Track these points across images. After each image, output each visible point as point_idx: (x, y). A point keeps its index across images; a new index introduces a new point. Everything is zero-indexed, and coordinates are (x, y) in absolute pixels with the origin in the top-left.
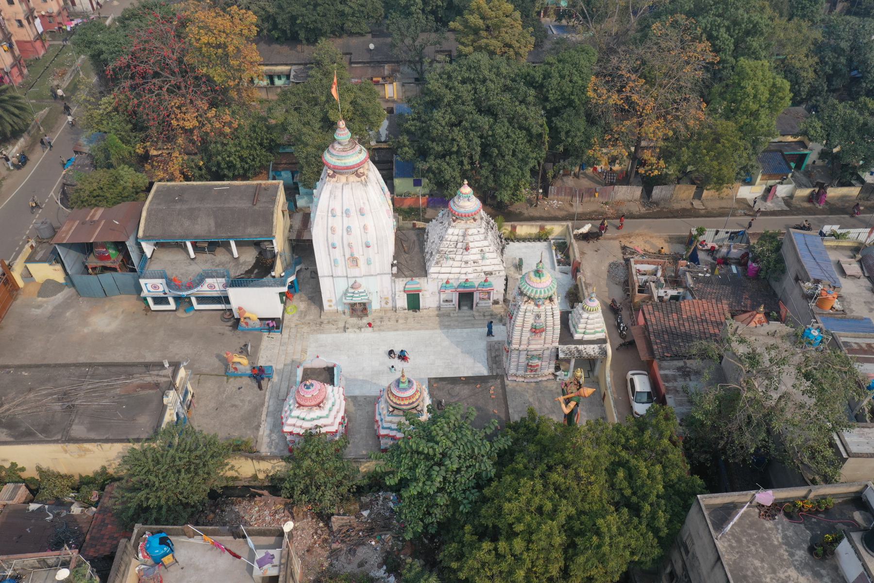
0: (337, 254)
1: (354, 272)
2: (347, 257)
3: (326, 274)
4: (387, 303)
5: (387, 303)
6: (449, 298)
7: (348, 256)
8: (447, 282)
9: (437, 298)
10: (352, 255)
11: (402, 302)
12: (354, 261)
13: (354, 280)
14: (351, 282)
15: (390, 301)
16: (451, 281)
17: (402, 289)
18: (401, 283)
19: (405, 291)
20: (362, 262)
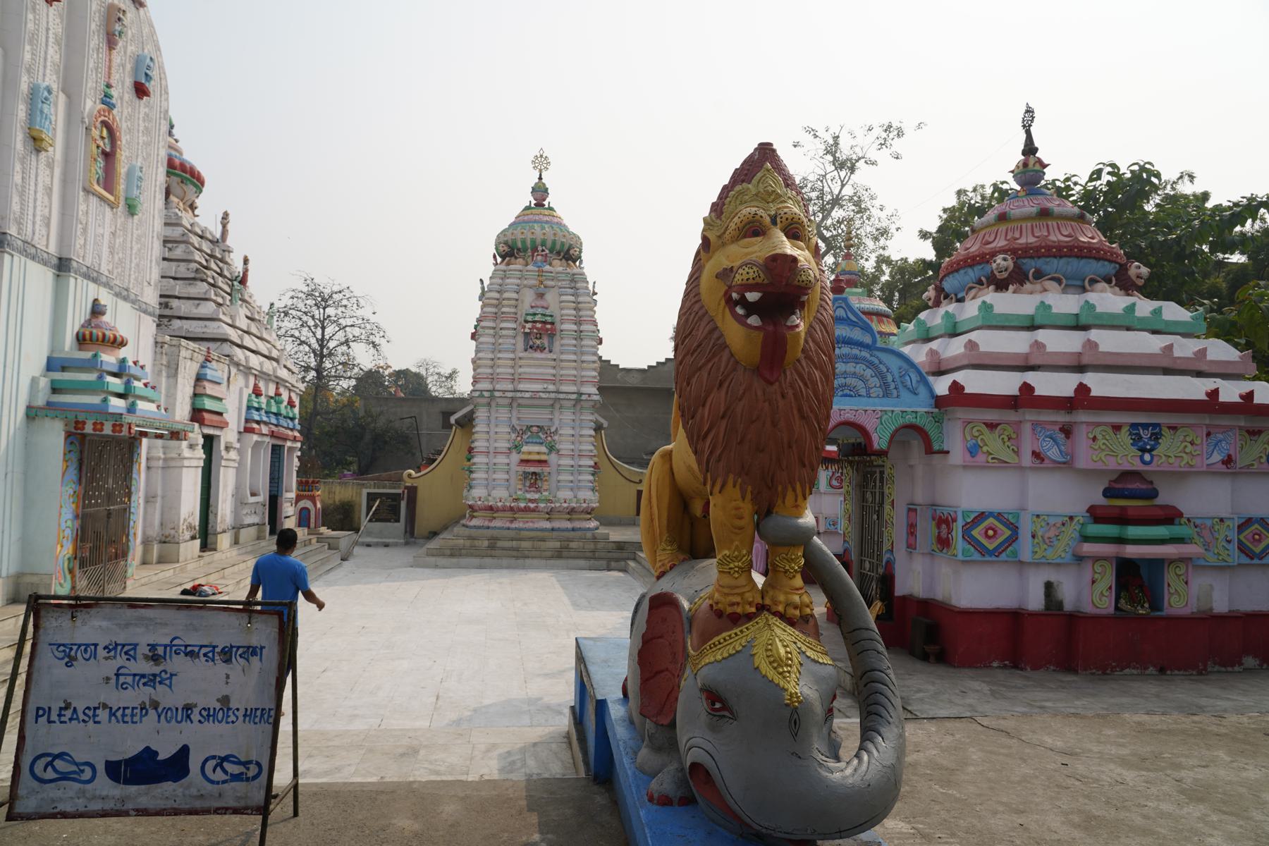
7: (90, 105)
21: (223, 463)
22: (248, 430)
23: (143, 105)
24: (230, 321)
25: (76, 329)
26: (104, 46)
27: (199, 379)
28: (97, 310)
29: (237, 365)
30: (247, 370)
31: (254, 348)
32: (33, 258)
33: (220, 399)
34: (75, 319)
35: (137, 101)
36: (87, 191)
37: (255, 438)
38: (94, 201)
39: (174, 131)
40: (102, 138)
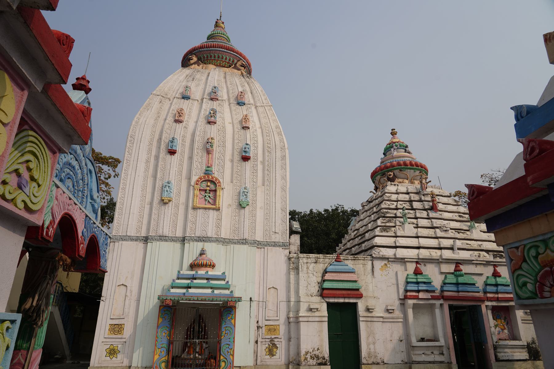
0: (174, 169)
1: (206, 222)
2: (194, 179)
3: (132, 232)
4: (271, 352)
5: (271, 352)
6: (428, 332)
8: (417, 272)
9: (397, 330)
10: (208, 172)
11: (315, 337)
12: (209, 186)
13: (200, 245)
14: (192, 251)
15: (282, 346)
16: (422, 267)
17: (315, 289)
18: (313, 267)
19: (322, 295)
20: (226, 197)
21: (361, 319)
22: (406, 297)
23: (248, 164)
24: (394, 235)
25: (191, 261)
26: (205, 154)
27: (325, 272)
28: (202, 253)
29: (383, 258)
30: (403, 261)
31: (416, 245)
32: (166, 241)
33: (356, 281)
34: (188, 260)
35: (244, 163)
36: (195, 208)
37: (411, 302)
38: (200, 212)
39: (409, 149)
40: (208, 186)
